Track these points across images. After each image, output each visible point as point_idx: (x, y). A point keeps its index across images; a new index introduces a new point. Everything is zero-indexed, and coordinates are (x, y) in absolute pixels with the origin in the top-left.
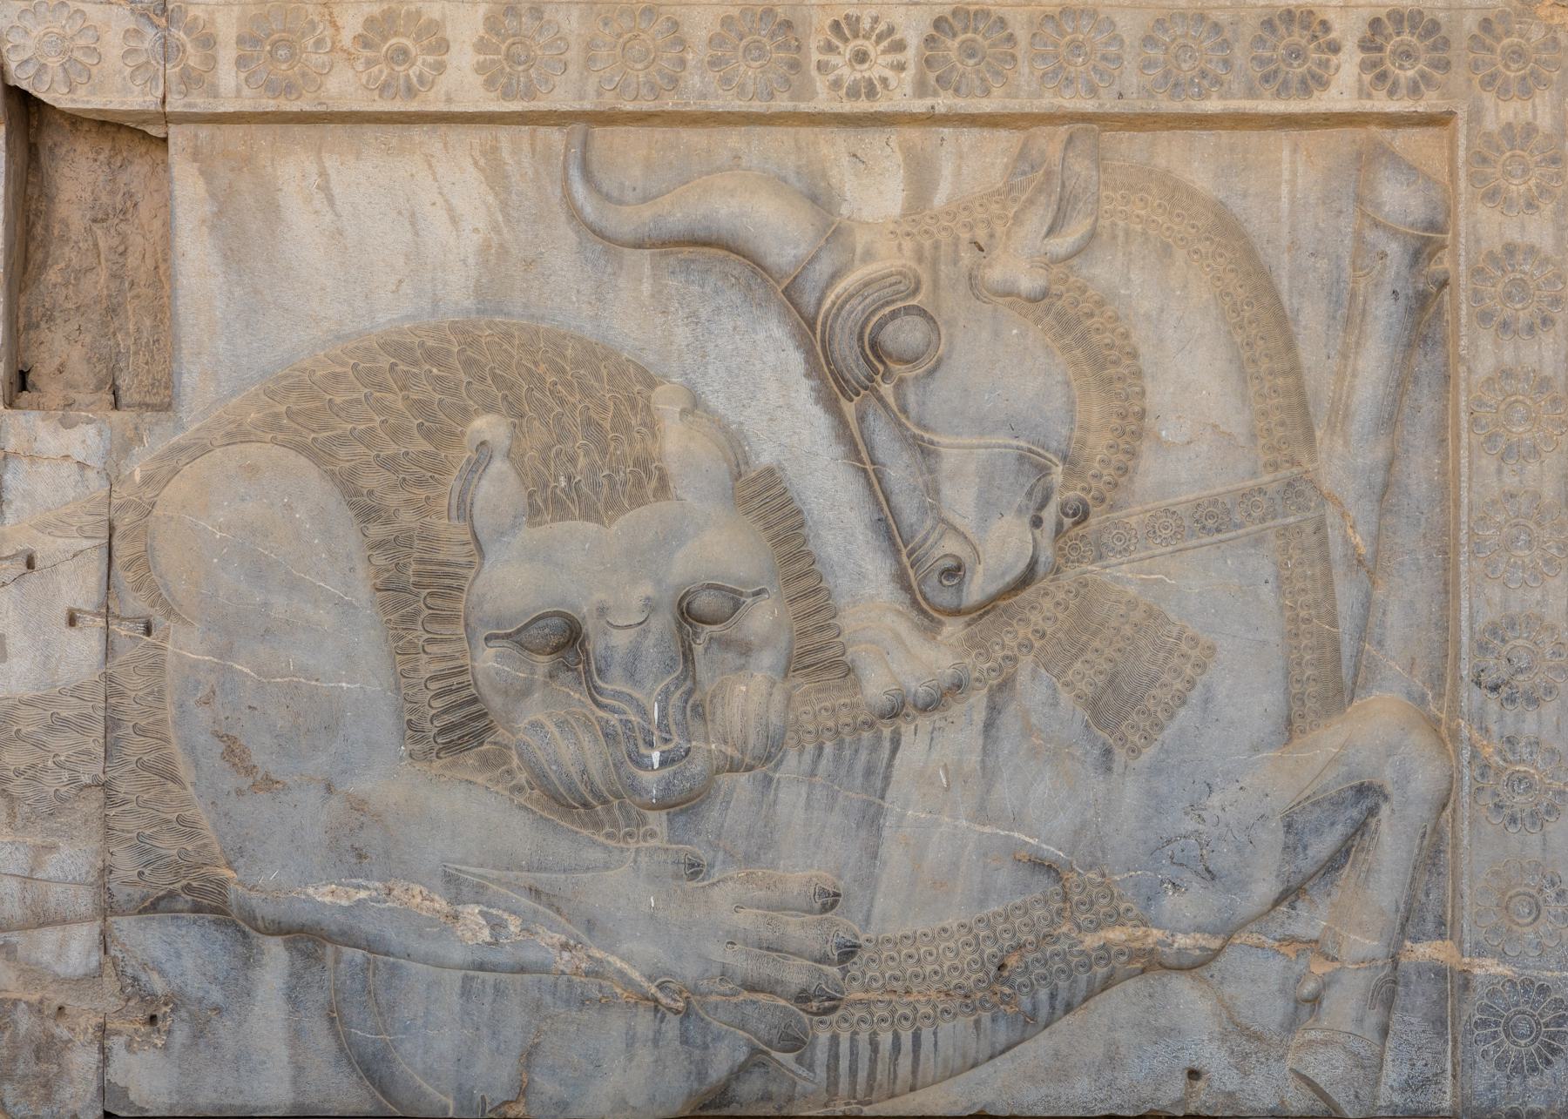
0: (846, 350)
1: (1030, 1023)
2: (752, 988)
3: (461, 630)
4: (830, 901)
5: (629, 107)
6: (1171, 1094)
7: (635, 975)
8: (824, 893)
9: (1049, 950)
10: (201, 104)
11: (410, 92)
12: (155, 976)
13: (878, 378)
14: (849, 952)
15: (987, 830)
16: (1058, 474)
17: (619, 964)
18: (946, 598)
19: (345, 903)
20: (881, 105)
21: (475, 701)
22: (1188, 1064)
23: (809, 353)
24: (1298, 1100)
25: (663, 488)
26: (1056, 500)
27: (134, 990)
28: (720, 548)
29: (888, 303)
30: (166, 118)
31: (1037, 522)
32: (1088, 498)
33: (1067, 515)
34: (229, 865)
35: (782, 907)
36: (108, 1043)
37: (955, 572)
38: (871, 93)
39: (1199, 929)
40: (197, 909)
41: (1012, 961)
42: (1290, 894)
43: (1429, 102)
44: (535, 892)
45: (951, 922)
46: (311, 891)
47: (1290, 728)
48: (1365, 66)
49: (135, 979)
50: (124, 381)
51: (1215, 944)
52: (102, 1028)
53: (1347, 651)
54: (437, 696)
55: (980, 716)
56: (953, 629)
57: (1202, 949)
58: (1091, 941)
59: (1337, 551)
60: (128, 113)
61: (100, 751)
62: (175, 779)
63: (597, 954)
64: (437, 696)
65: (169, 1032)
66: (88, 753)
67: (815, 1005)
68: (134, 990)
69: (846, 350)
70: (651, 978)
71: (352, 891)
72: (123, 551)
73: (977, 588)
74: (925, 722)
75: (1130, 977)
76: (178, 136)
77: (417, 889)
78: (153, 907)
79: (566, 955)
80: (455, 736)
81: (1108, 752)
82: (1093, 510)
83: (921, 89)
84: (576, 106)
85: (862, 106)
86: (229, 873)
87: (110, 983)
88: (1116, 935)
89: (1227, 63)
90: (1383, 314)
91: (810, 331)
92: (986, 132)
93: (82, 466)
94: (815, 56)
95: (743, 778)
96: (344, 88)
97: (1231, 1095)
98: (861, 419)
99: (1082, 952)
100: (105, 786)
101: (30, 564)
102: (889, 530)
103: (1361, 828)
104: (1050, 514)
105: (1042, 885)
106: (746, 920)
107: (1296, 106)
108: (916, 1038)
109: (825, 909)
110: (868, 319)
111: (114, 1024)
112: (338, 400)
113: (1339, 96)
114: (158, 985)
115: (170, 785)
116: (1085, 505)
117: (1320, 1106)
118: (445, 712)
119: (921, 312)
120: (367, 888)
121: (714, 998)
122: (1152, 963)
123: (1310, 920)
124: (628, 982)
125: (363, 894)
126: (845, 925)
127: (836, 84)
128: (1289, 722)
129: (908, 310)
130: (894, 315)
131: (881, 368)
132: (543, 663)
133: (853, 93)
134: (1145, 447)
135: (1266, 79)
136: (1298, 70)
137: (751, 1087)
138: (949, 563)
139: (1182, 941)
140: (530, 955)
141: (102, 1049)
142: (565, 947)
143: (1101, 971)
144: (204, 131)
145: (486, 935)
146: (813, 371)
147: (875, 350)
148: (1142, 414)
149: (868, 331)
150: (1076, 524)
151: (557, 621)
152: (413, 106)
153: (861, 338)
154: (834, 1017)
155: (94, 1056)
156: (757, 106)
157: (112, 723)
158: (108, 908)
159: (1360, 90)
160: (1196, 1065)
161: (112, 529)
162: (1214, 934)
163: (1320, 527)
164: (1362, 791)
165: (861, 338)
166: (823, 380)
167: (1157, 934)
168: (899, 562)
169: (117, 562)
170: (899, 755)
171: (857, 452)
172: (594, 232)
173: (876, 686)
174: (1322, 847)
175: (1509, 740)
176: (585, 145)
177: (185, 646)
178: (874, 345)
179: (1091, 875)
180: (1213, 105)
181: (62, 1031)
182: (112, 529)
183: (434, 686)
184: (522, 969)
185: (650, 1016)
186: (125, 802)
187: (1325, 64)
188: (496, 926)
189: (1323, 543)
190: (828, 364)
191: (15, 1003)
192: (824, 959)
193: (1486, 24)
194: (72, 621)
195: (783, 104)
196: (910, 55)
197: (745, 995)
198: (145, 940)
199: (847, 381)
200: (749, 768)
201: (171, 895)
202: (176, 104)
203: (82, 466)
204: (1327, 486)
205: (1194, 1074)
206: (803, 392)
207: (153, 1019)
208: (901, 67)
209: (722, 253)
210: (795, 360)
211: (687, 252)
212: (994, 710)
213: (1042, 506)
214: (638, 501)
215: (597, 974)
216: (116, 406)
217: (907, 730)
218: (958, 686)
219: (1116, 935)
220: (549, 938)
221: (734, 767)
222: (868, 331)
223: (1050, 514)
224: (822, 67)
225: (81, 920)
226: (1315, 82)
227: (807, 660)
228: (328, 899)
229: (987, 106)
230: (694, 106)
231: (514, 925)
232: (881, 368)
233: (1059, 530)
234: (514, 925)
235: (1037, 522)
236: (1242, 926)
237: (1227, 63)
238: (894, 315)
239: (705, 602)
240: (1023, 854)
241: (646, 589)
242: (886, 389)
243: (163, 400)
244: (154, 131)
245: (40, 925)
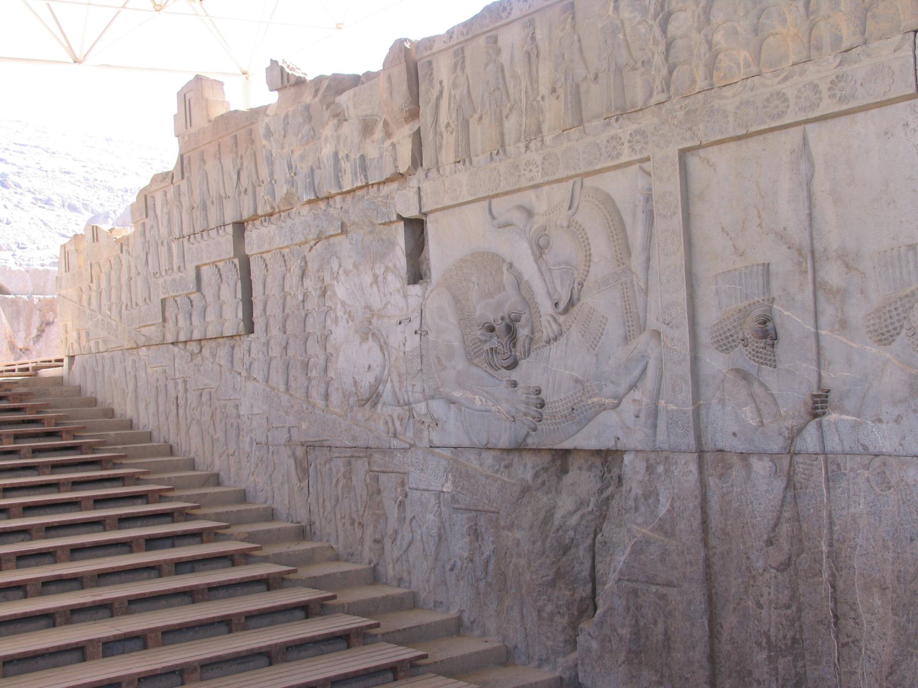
25: (504, 289)
43: (645, 155)
44: (487, 392)
45: (562, 397)
47: (626, 339)
48: (630, 147)
51: (616, 402)
53: (641, 315)
58: (590, 402)
59: (636, 288)
83: (542, 177)
84: (485, 195)
85: (532, 183)
88: (595, 400)
89: (601, 155)
90: (640, 216)
92: (561, 184)
96: (447, 202)
105: (579, 387)
107: (616, 162)
128: (626, 338)
134: (592, 264)
140: (488, 408)
162: (615, 398)
163: (632, 282)
164: (643, 356)
174: (636, 373)
175: (672, 339)
176: (490, 204)
177: (431, 337)
180: (598, 167)
188: (481, 400)
189: (633, 286)
193: (655, 129)
195: (517, 187)
196: (540, 168)
204: (633, 269)
214: (500, 292)
219: (595, 400)
226: (619, 155)
229: (554, 178)
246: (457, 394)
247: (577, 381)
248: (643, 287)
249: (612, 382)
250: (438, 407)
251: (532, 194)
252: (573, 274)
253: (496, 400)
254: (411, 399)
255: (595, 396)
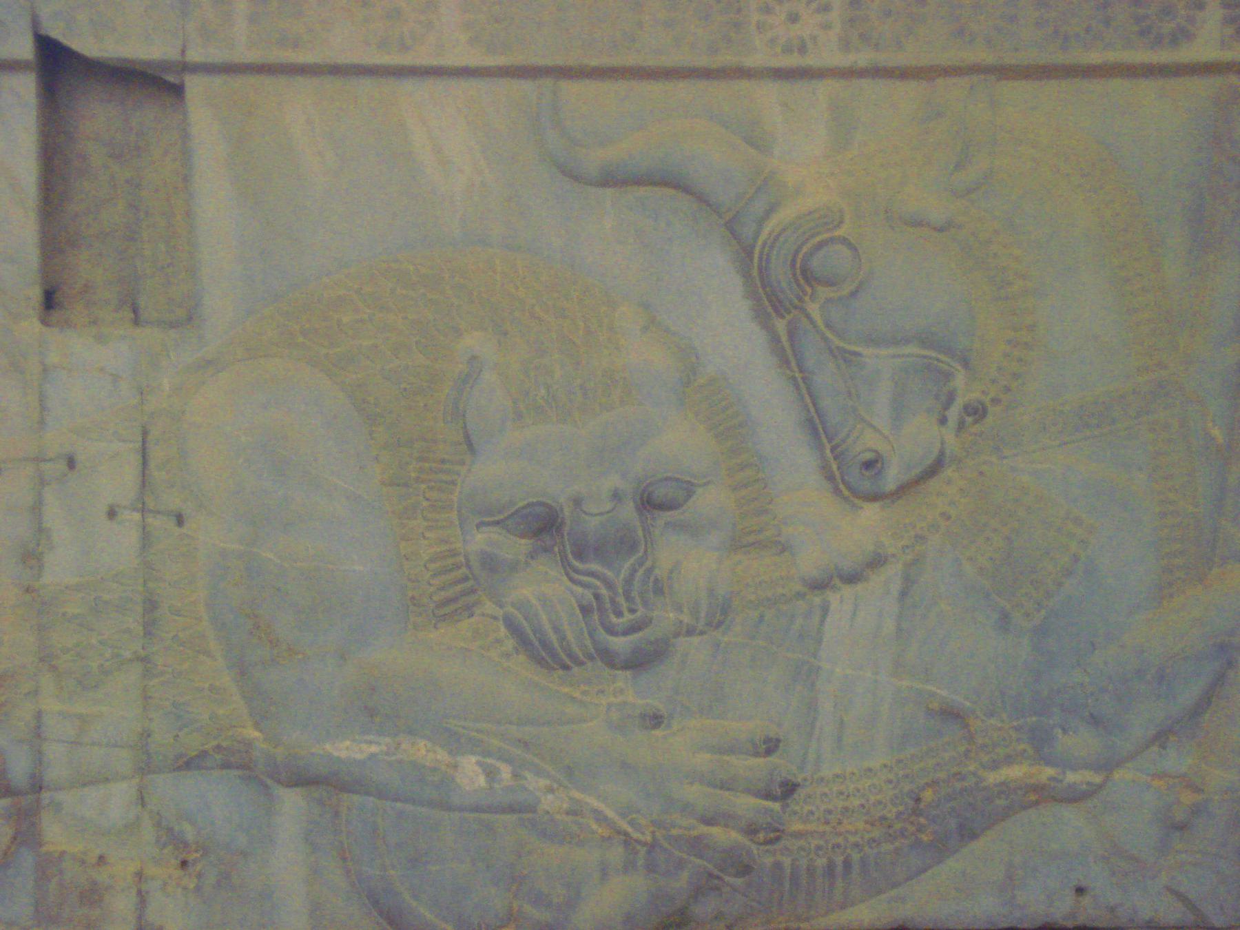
0: (780, 274)
1: (941, 849)
2: (709, 822)
3: (454, 516)
4: (771, 746)
5: (594, 63)
6: (1062, 908)
7: (610, 814)
8: (767, 740)
9: (958, 785)
10: (216, 55)
11: (404, 48)
12: (187, 827)
13: (807, 298)
14: (789, 789)
15: (905, 683)
16: (960, 380)
17: (595, 803)
18: (866, 486)
19: (359, 756)
20: (810, 61)
21: (466, 579)
22: (1075, 883)
23: (747, 275)
24: (1172, 912)
26: (959, 403)
27: (171, 838)
28: (679, 442)
29: (813, 236)
30: (187, 68)
31: (943, 421)
32: (987, 400)
33: (969, 415)
34: (257, 726)
35: (732, 750)
36: (144, 887)
37: (871, 464)
38: (802, 49)
39: (1087, 766)
40: (226, 766)
41: (928, 795)
42: (1161, 737)
46: (328, 746)
49: (170, 830)
50: (142, 302)
51: (1098, 779)
52: (140, 876)
54: (434, 576)
55: (895, 588)
56: (871, 513)
57: (1088, 784)
58: (992, 778)
60: (149, 63)
61: (140, 630)
62: (208, 654)
63: (577, 795)
64: (434, 576)
65: (200, 876)
66: (128, 631)
67: (761, 836)
68: (171, 838)
69: (780, 274)
70: (623, 815)
71: (364, 746)
72: (157, 454)
73: (892, 477)
74: (847, 591)
75: (1025, 808)
76: (195, 86)
77: (422, 743)
78: (188, 764)
79: (550, 797)
80: (447, 610)
81: (1005, 617)
82: (991, 409)
83: (846, 45)
85: (793, 61)
86: (257, 734)
87: (148, 832)
91: (750, 261)
93: (116, 378)
94: (755, 17)
95: (695, 640)
96: (343, 44)
97: (1112, 910)
98: (792, 335)
99: (985, 788)
100: (144, 660)
101: (71, 463)
102: (816, 427)
103: (1219, 680)
104: (954, 413)
106: (703, 760)
108: (847, 864)
109: (769, 752)
110: (800, 247)
111: (151, 870)
112: (345, 320)
113: (1204, 49)
114: (189, 832)
115: (202, 657)
116: (983, 404)
117: (1191, 917)
118: (443, 589)
119: (844, 241)
120: (378, 743)
121: (674, 832)
122: (1042, 795)
123: (1177, 760)
124: (600, 817)
125: (374, 749)
126: (782, 765)
127: (773, 41)
129: (832, 240)
130: (820, 245)
131: (809, 290)
132: (525, 544)
133: (788, 50)
135: (1142, 33)
136: (1168, 27)
137: (705, 908)
138: (869, 456)
139: (1071, 777)
141: (139, 892)
142: (551, 790)
143: (1001, 802)
144: (217, 81)
145: (482, 781)
146: (751, 294)
147: (807, 276)
148: (1031, 328)
149: (800, 256)
150: (976, 422)
151: (539, 510)
152: (407, 60)
153: (793, 265)
154: (778, 846)
155: (134, 898)
156: (703, 61)
157: (151, 605)
158: (145, 767)
159: (1223, 42)
160: (1083, 884)
161: (145, 433)
162: (1097, 767)
164: (1222, 648)
165: (793, 265)
166: (759, 299)
167: (1050, 771)
168: (823, 457)
169: (152, 464)
170: (828, 620)
171: (787, 362)
172: (563, 173)
173: (809, 561)
174: (1189, 694)
178: (804, 272)
179: (993, 721)
181: (102, 876)
182: (145, 433)
183: (432, 566)
184: (511, 809)
185: (621, 849)
186: (162, 673)
187: (1191, 20)
188: (491, 774)
190: (764, 287)
191: (63, 853)
192: (768, 796)
194: (112, 514)
195: (726, 58)
196: (835, 16)
197: (704, 829)
198: (174, 791)
199: (780, 302)
200: (702, 633)
201: (203, 754)
202: (194, 56)
203: (116, 378)
205: (1080, 891)
206: (742, 307)
207: (184, 864)
208: (826, 27)
209: (672, 192)
210: (736, 282)
211: (642, 191)
212: (908, 582)
213: (946, 409)
215: (575, 813)
216: (136, 322)
217: (833, 598)
218: (877, 561)
219: (1015, 772)
220: (535, 783)
221: (690, 632)
222: (800, 256)
223: (954, 413)
224: (760, 27)
225: (124, 778)
226: (1182, 35)
227: (751, 539)
228: (343, 754)
230: (652, 62)
231: (506, 772)
232: (809, 290)
233: (961, 426)
234: (506, 772)
235: (943, 421)
236: (1119, 764)
237: (1107, 22)
238: (820, 245)
239: (660, 493)
240: (935, 705)
241: (614, 481)
242: (814, 309)
243: (187, 318)
244: (171, 78)
245: (84, 785)
246: (349, 749)
247: (951, 714)
248: (1221, 440)
249: (1095, 721)
250: (213, 801)
251: (768, 95)
252: (948, 376)
253: (569, 771)
254: (56, 772)
255: (1009, 760)
